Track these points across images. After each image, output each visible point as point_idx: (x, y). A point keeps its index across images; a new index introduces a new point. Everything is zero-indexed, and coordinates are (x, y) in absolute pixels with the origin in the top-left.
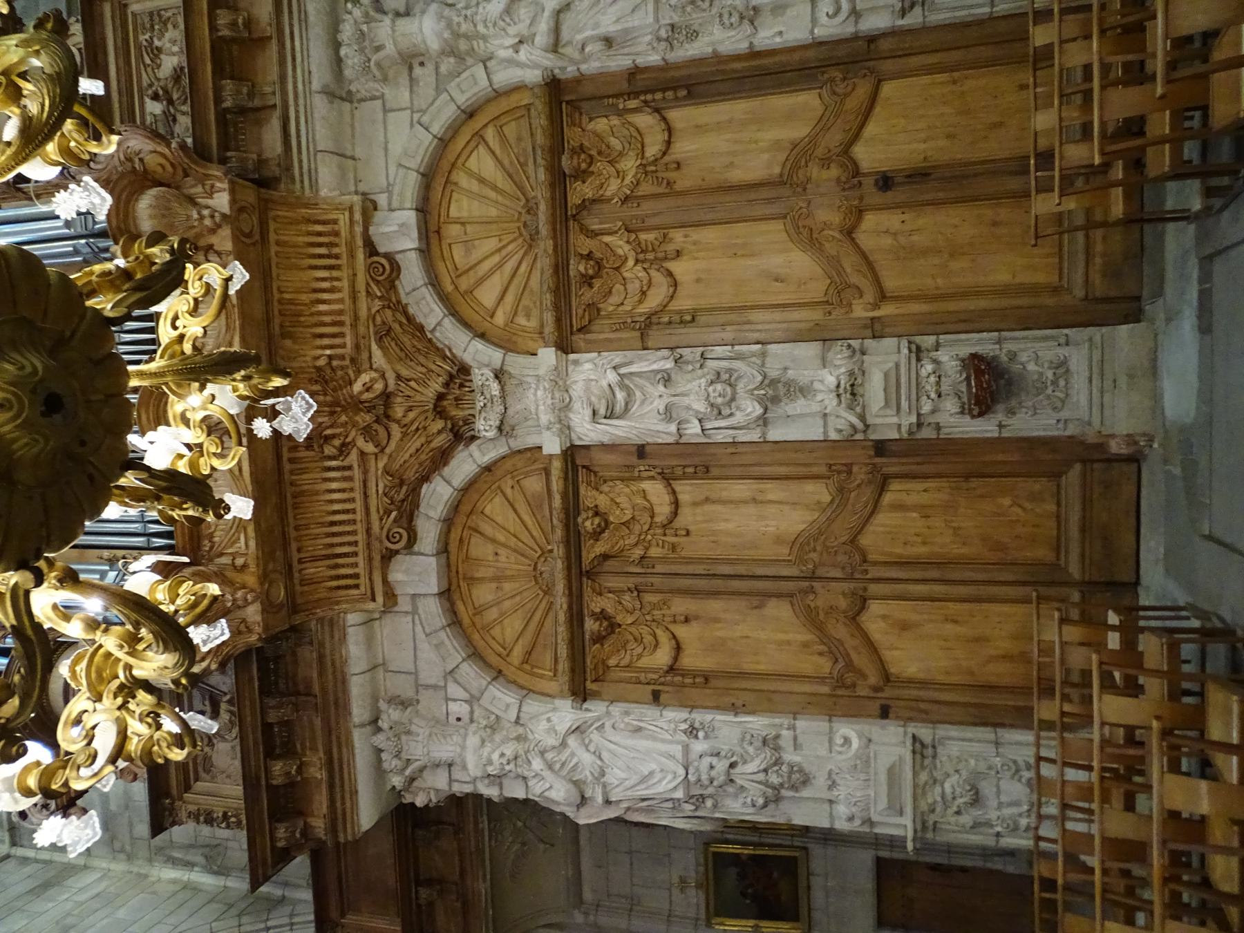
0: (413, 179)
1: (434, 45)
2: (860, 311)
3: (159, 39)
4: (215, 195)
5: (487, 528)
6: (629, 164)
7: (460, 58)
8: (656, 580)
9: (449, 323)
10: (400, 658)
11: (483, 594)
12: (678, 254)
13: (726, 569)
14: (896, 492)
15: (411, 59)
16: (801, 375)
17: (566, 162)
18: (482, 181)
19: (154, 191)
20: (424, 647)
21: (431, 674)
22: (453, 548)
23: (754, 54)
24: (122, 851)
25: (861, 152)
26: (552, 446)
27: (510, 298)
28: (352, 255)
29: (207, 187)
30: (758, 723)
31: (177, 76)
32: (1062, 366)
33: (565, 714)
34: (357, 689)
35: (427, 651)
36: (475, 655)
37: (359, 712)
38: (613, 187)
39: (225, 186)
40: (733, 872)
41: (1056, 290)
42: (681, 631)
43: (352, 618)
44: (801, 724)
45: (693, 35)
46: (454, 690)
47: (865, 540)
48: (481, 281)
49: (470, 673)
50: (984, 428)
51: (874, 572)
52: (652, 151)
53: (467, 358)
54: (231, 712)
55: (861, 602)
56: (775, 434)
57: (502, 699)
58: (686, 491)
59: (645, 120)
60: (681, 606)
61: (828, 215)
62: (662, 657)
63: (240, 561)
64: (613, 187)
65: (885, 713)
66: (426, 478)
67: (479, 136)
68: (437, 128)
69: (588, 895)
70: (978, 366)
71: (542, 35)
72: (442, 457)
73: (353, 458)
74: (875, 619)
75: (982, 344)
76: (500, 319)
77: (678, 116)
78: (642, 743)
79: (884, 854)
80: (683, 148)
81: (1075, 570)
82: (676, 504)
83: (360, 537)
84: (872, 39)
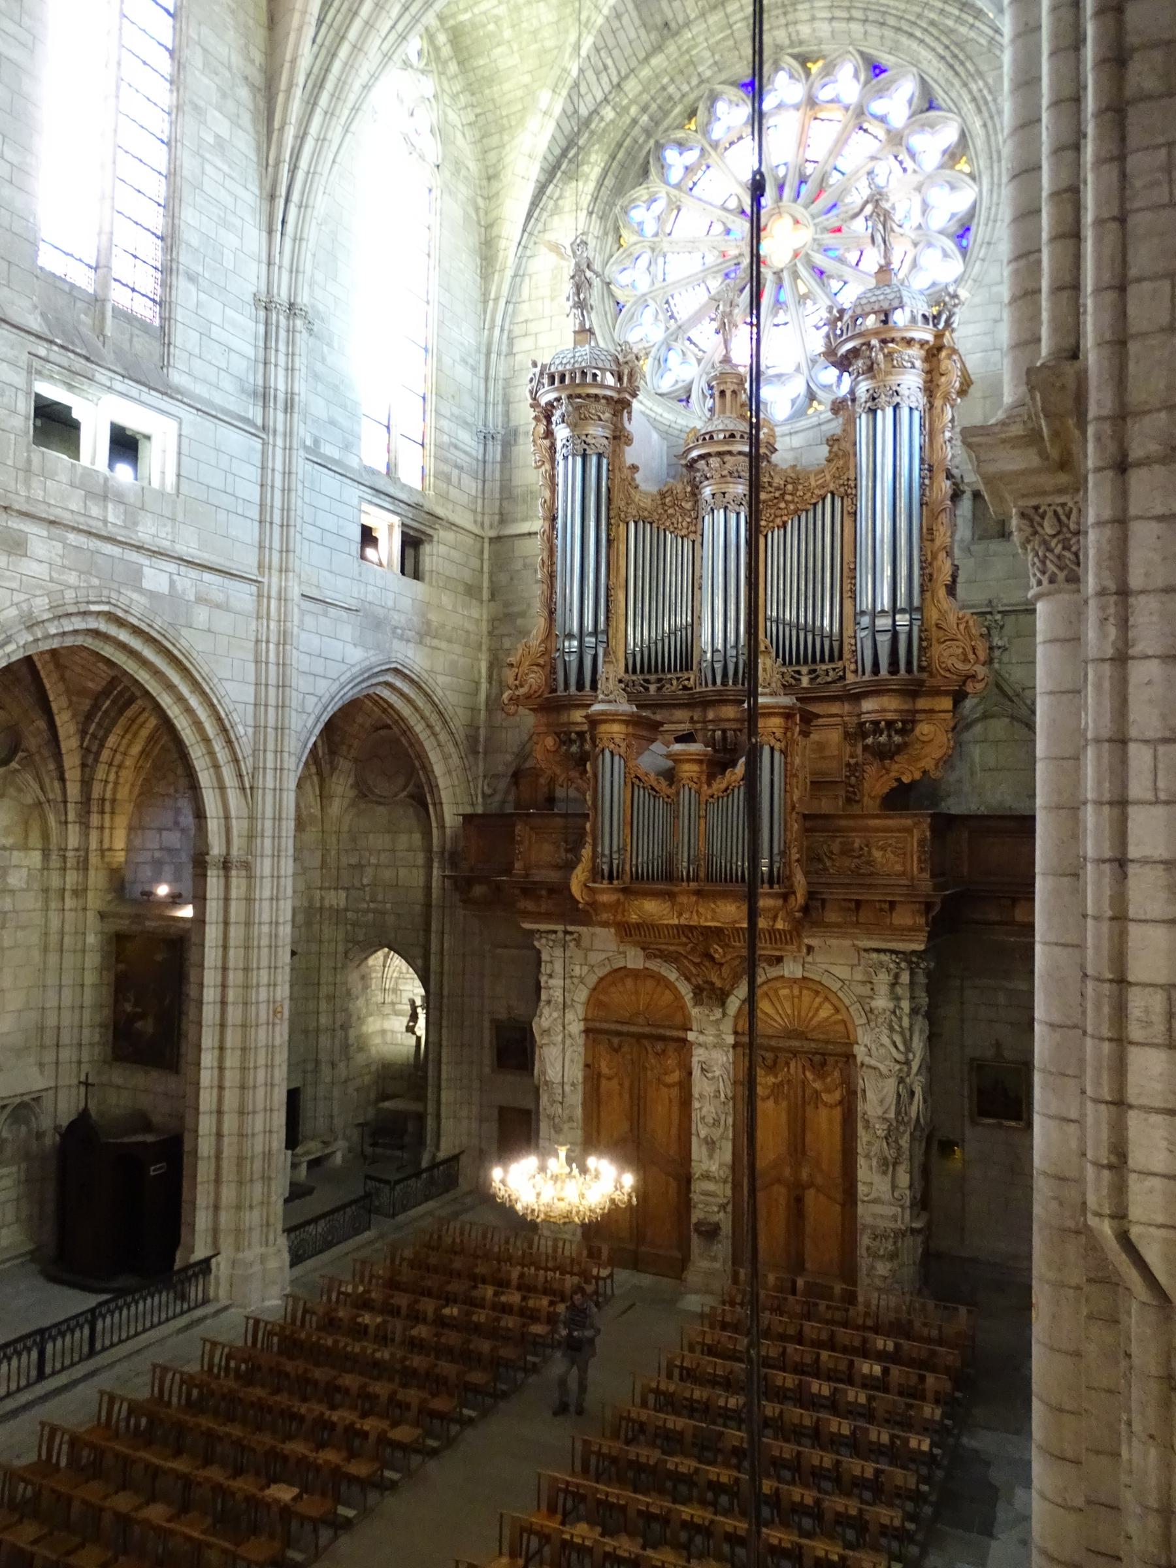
1: (874, 1004)
6: (817, 1085)
12: (776, 1102)
18: (817, 1010)
20: (603, 956)
24: (494, 628)
30: (579, 1112)
31: (869, 863)
32: (714, 1259)
36: (601, 979)
37: (570, 928)
42: (615, 1082)
49: (592, 980)
57: (582, 995)
58: (675, 1092)
59: (837, 1095)
62: (605, 1070)
66: (678, 969)
67: (837, 1011)
69: (499, 951)
71: (867, 1060)
73: (684, 940)
75: (726, 1228)
77: (837, 1113)
81: (643, 1249)
82: (669, 1086)
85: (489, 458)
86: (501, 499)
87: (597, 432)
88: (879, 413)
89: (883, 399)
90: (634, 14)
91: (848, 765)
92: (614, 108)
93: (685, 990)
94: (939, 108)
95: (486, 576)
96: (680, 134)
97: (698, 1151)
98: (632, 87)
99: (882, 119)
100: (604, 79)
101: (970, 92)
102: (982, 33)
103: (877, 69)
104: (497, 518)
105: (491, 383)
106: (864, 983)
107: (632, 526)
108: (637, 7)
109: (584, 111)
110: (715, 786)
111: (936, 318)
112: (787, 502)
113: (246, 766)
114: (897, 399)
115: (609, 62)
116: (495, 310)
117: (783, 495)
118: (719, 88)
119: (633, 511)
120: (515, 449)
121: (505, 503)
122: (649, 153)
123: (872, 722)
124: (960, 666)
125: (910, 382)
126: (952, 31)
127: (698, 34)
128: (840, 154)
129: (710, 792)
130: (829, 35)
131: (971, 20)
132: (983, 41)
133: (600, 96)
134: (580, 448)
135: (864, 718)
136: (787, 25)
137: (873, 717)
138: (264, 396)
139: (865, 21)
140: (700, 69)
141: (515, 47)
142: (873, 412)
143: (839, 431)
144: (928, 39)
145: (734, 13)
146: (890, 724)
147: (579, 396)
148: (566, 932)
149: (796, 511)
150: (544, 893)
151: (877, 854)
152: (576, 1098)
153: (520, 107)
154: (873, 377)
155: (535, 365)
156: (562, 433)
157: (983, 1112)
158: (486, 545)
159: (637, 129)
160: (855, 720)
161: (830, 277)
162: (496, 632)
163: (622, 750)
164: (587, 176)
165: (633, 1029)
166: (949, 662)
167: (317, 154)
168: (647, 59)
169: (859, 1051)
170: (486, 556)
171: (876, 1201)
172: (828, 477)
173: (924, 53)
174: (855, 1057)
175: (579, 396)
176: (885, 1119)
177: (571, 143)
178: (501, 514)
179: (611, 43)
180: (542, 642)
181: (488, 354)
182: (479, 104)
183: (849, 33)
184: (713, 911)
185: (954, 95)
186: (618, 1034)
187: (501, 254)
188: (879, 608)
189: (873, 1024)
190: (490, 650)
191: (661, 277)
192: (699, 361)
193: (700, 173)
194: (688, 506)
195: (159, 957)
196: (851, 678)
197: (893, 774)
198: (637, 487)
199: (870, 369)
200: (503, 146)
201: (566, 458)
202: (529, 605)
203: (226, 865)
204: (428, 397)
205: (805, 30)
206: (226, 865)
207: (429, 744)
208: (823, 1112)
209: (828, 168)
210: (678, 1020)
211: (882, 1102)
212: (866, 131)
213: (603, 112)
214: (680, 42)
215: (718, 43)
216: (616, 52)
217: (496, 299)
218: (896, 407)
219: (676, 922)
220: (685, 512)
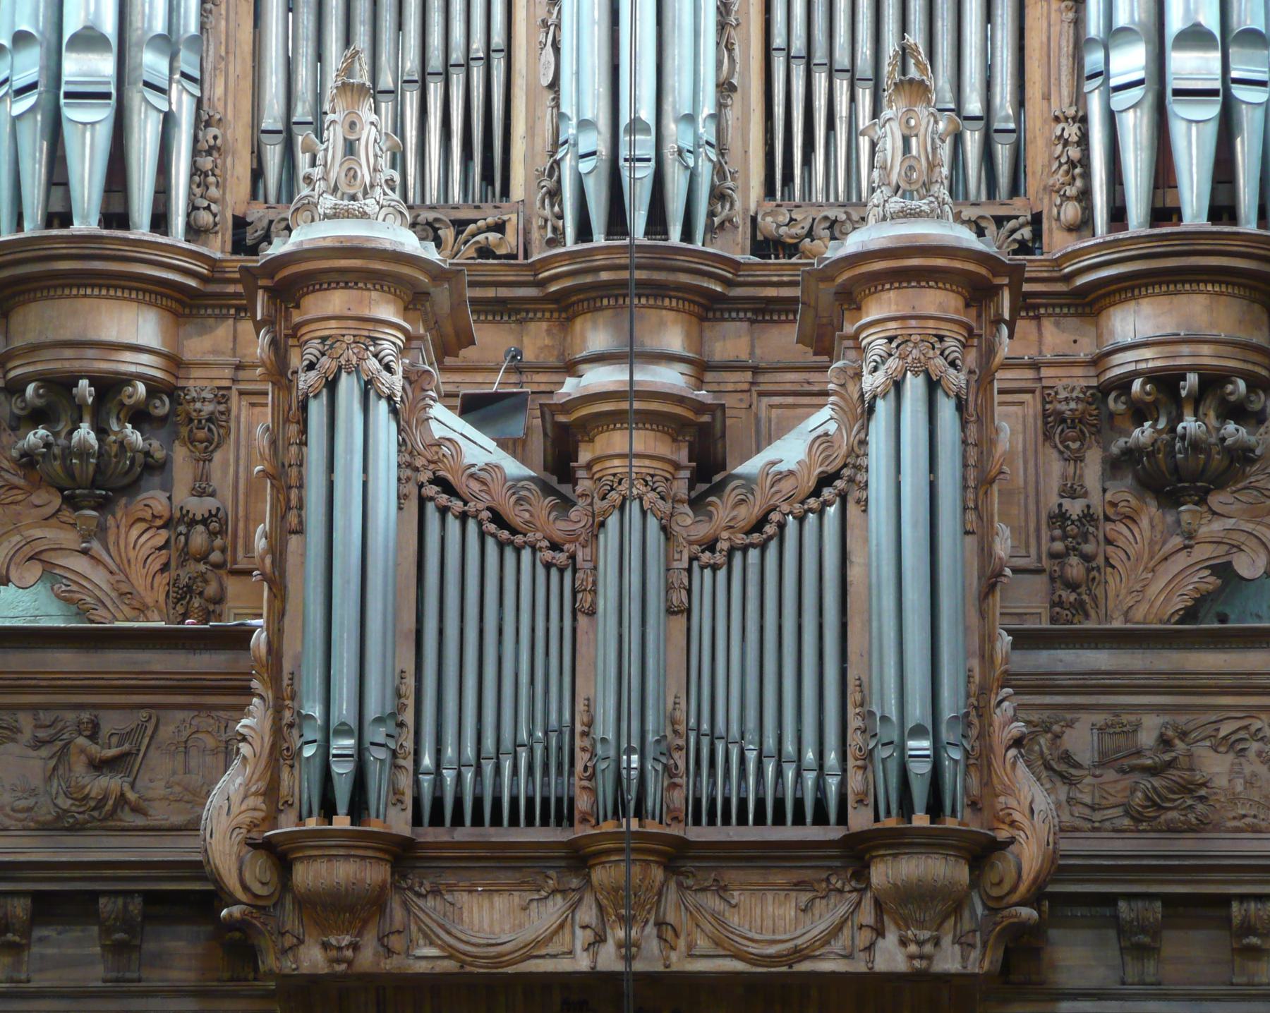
3: (1259, 754)
4: (957, 947)
19: (965, 871)
29: (970, 939)
39: (973, 968)
54: (105, 799)
63: (395, 942)
91: (1060, 517)
123: (1153, 377)
129: (703, 530)
135: (1122, 364)
137: (1150, 359)
146: (1212, 381)
160: (1081, 379)
163: (395, 382)
188: (1175, 24)
196: (1058, 243)
197: (1202, 552)
219: (582, 963)
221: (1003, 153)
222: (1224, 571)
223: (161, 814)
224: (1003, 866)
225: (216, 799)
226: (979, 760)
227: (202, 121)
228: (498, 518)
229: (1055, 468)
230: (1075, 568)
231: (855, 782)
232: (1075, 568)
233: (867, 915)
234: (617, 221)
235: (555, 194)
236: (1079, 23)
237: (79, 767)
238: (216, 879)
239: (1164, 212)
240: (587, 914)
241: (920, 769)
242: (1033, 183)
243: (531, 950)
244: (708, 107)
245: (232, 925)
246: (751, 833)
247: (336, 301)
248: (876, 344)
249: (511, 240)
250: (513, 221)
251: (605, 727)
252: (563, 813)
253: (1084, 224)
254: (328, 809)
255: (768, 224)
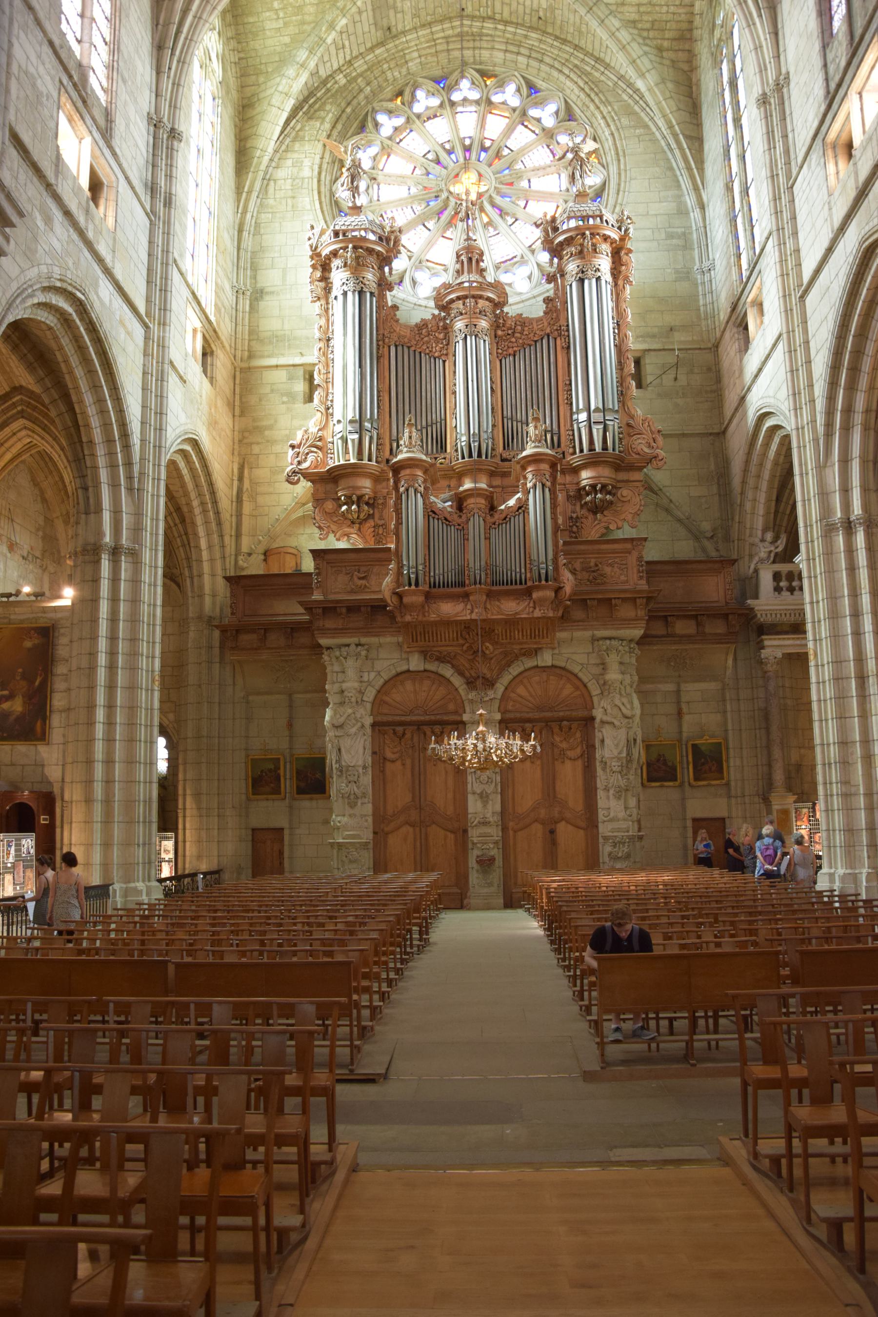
0: (563, 664)
2: (511, 824)
5: (434, 687)
6: (564, 745)
7: (605, 684)
8: (417, 754)
9: (511, 677)
10: (383, 654)
11: (409, 686)
13: (422, 779)
14: (451, 836)
15: (604, 666)
16: (490, 806)
17: (565, 723)
21: (379, 666)
22: (426, 674)
23: (596, 789)
25: (563, 823)
26: (466, 717)
27: (519, 699)
28: (536, 643)
32: (490, 885)
33: (368, 721)
34: (374, 640)
35: (386, 663)
36: (386, 682)
37: (364, 640)
38: (558, 739)
40: (272, 767)
41: (516, 884)
42: (399, 763)
43: (400, 639)
44: (370, 806)
45: (604, 769)
46: (373, 675)
47: (434, 826)
48: (525, 687)
50: (472, 863)
51: (423, 830)
52: (570, 754)
53: (498, 685)
55: (412, 825)
56: (471, 798)
57: (370, 694)
59: (578, 751)
60: (408, 762)
61: (543, 812)
62: (389, 755)
64: (558, 739)
65: (375, 833)
66: (453, 666)
67: (577, 688)
68: (580, 675)
69: (251, 698)
70: (492, 860)
71: (605, 718)
72: (461, 674)
73: (461, 641)
74: (406, 829)
75: (499, 862)
76: (513, 695)
77: (579, 763)
78: (361, 751)
79: (286, 832)
80: (568, 764)
83: (431, 643)
84: (597, 827)
85: (240, 307)
86: (249, 340)
87: (370, 276)
88: (586, 282)
89: (590, 272)
90: (371, 13)
91: (572, 518)
92: (345, 76)
93: (457, 681)
94: (575, 120)
95: (237, 397)
96: (391, 105)
97: (474, 806)
98: (359, 64)
99: (539, 120)
100: (341, 55)
101: (601, 113)
102: (609, 78)
103: (532, 88)
104: (246, 353)
105: (242, 253)
106: (598, 665)
107: (393, 349)
108: (373, 10)
109: (323, 73)
110: (496, 516)
111: (620, 228)
112: (517, 338)
113: (136, 469)
114: (599, 274)
115: (347, 43)
116: (247, 200)
117: (513, 333)
118: (420, 80)
119: (395, 337)
120: (262, 304)
121: (253, 343)
122: (367, 114)
123: (590, 485)
124: (646, 450)
125: (604, 264)
126: (590, 74)
127: (410, 41)
128: (509, 138)
129: (492, 520)
130: (502, 62)
131: (602, 69)
132: (610, 84)
133: (335, 66)
134: (358, 288)
135: (584, 483)
136: (474, 48)
137: (590, 482)
138: (152, 189)
139: (529, 57)
140: (410, 64)
141: (281, 15)
142: (581, 281)
143: (551, 293)
144: (572, 75)
145: (437, 32)
146: (604, 486)
147: (361, 248)
148: (357, 645)
149: (523, 345)
150: (344, 610)
151: (608, 570)
152: (367, 780)
153: (277, 59)
154: (583, 258)
155: (312, 227)
156: (339, 276)
157: (650, 779)
158: (238, 373)
159: (361, 97)
160: (575, 487)
161: (507, 214)
162: (245, 441)
163: (422, 489)
164: (323, 119)
165: (414, 718)
166: (639, 448)
167: (194, 27)
168: (372, 49)
169: (598, 714)
170: (237, 382)
171: (611, 820)
172: (546, 324)
173: (568, 83)
174: (593, 719)
175: (361, 248)
176: (619, 759)
177: (311, 94)
178: (249, 351)
179: (351, 30)
180: (319, 430)
181: (240, 231)
182: (243, 51)
183: (516, 62)
184: (499, 607)
185: (588, 114)
186: (402, 724)
187: (256, 159)
188: (593, 407)
189: (606, 693)
190: (239, 454)
191: (375, 198)
192: (410, 258)
193: (405, 134)
194: (441, 336)
195: (28, 644)
198: (397, 321)
199: (581, 252)
200: (259, 85)
201: (345, 294)
202: (276, 421)
203: (115, 552)
204: (210, 246)
205: (485, 54)
206: (115, 552)
207: (199, 520)
208: (568, 764)
209: (502, 144)
210: (451, 707)
211: (617, 745)
212: (526, 127)
213: (337, 78)
214: (397, 42)
215: (424, 48)
216: (352, 38)
217: (249, 192)
218: (598, 279)
219: (468, 617)
220: (437, 340)
221: (555, 438)
222: (607, 528)
223: (373, 589)
224: (562, 593)
225: (384, 583)
226: (556, 569)
227: (378, 439)
228: (446, 519)
229: (570, 507)
230: (575, 529)
231: (528, 575)
232: (575, 529)
233: (532, 605)
234: (470, 456)
235: (457, 450)
236: (571, 409)
237: (355, 579)
238: (385, 601)
239: (592, 448)
240: (469, 607)
241: (543, 572)
242: (562, 445)
243: (456, 615)
244: (490, 430)
245: (390, 611)
246: (505, 587)
247: (408, 471)
248: (530, 476)
249: (448, 461)
250: (448, 456)
251: (471, 565)
252: (463, 584)
253: (575, 453)
254: (410, 585)
255: (504, 456)
